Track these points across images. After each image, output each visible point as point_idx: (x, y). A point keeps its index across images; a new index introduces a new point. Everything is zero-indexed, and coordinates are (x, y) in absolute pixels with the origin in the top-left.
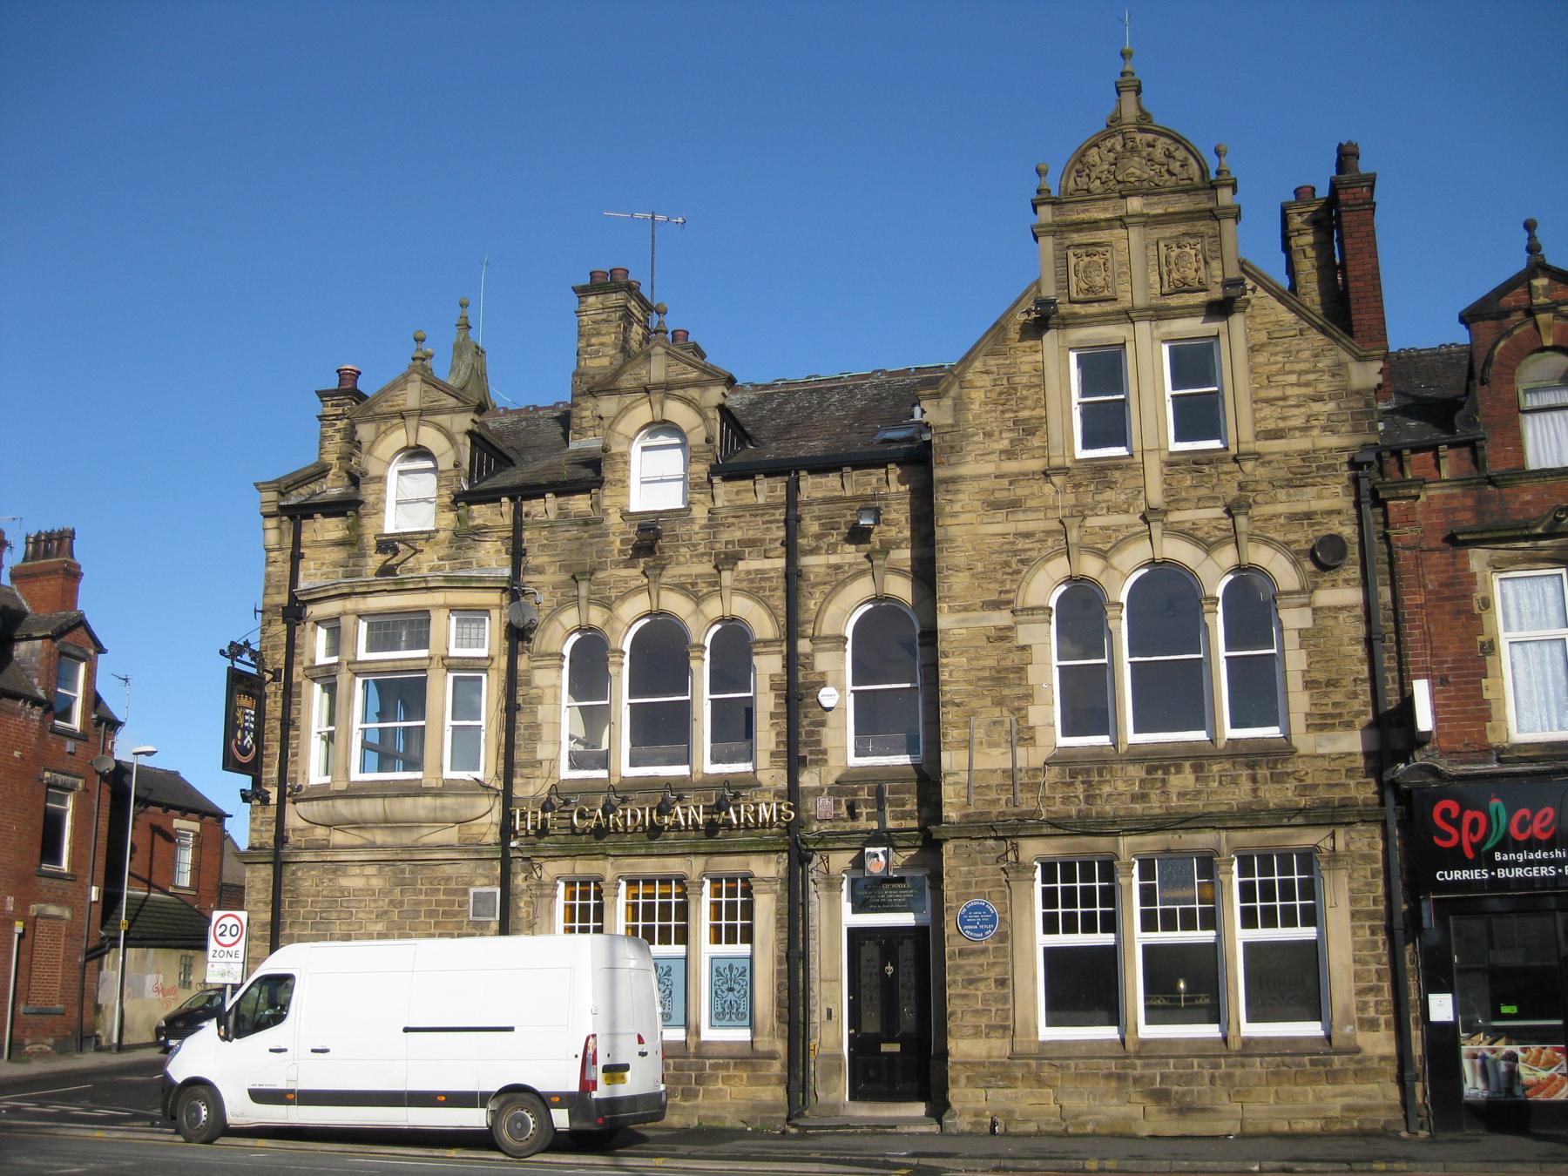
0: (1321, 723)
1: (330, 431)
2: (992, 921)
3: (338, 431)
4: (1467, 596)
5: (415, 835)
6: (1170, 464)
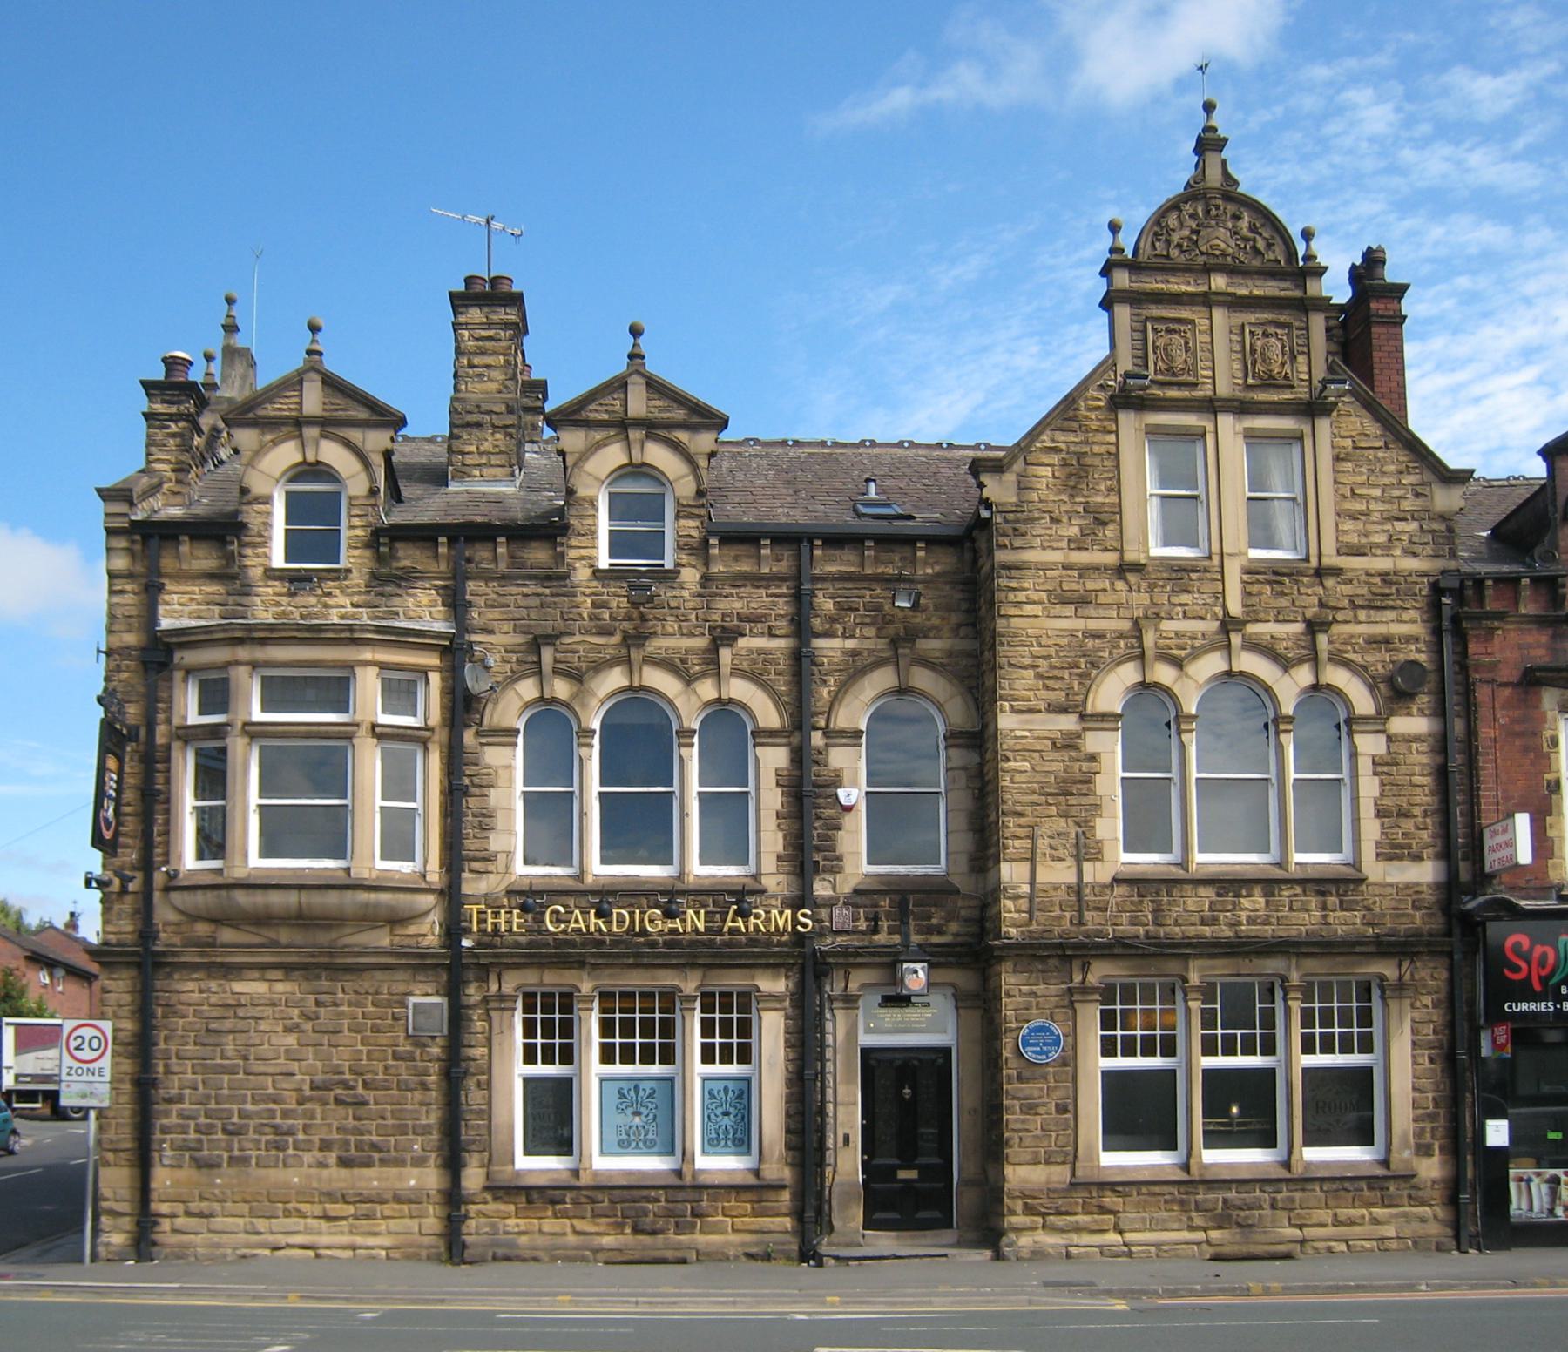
0: (1391, 851)
1: (160, 435)
2: (1057, 1042)
3: (174, 435)
4: (1536, 734)
5: (334, 935)
6: (1248, 572)
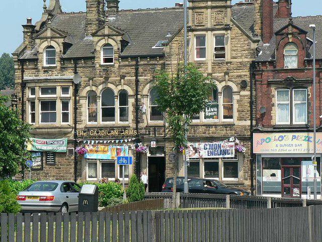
0: (240, 119)
3: (29, 36)
